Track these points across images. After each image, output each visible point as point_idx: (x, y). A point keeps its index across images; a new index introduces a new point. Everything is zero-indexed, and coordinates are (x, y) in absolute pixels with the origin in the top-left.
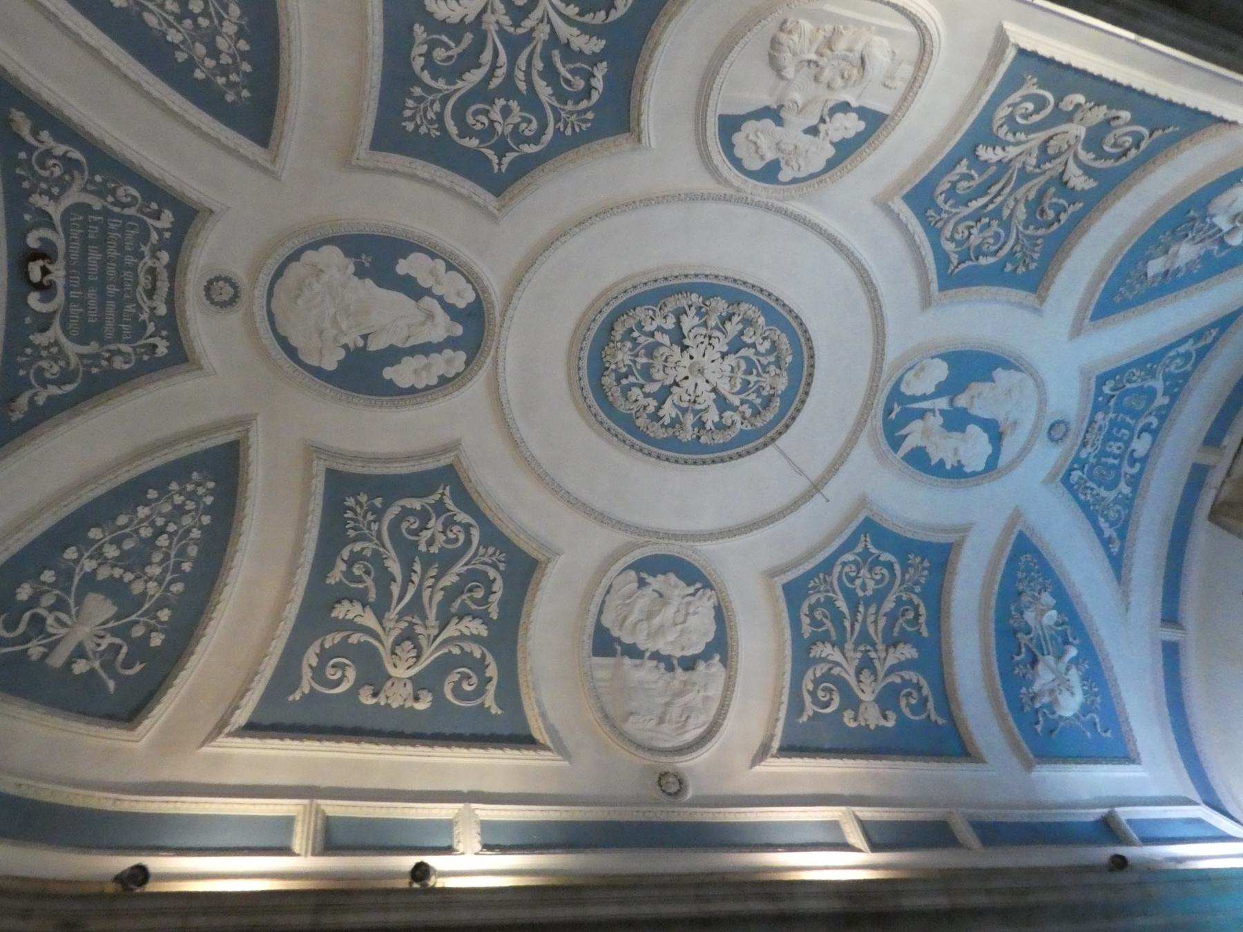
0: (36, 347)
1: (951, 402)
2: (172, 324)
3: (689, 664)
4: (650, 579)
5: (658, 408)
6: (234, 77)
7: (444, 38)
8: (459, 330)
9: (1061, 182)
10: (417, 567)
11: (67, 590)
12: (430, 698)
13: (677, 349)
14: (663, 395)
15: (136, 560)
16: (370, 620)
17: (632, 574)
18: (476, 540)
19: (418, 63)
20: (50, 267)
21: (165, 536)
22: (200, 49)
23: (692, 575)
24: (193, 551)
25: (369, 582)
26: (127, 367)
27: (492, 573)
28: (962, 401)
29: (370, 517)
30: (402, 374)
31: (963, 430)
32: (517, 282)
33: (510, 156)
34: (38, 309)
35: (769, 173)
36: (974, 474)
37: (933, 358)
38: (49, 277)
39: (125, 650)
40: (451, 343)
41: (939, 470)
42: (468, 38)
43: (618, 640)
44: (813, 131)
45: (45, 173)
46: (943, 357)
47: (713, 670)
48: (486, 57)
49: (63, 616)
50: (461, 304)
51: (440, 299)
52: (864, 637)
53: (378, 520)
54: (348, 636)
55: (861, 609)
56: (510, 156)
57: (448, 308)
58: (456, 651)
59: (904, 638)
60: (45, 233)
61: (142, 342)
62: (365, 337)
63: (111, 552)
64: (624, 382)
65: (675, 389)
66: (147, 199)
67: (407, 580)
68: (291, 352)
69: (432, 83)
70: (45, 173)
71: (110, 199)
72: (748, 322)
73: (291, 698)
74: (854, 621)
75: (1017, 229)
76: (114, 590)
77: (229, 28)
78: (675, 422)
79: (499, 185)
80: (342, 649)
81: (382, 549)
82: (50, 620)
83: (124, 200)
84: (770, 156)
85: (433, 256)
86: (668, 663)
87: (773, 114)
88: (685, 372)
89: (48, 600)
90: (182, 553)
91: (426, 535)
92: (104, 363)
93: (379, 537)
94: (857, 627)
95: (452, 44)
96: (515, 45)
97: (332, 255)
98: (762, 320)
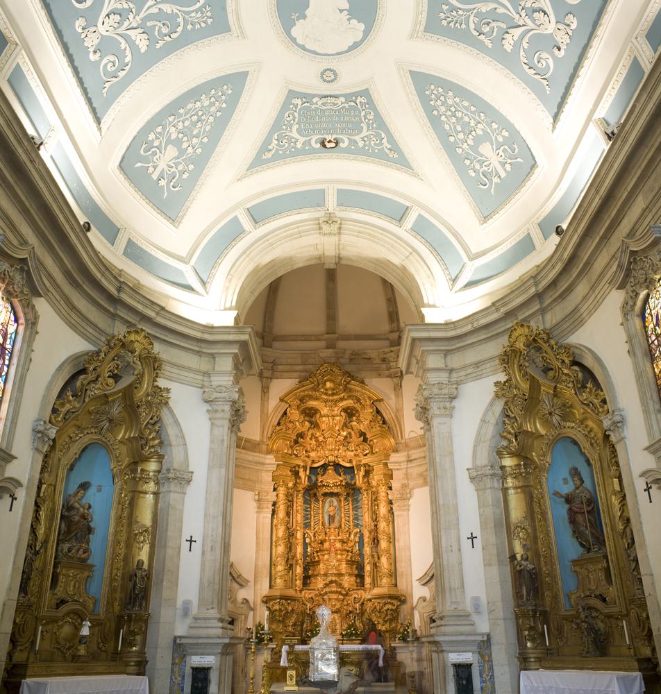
0: (365, 146)
2: (349, 97)
6: (220, 94)
7: (156, 33)
11: (475, 158)
12: (571, 16)
15: (468, 130)
20: (328, 140)
21: (457, 112)
22: (213, 109)
24: (466, 104)
25: (493, 24)
26: (372, 114)
29: (455, 13)
34: (347, 144)
38: (332, 140)
39: (507, 147)
42: (149, 24)
45: (287, 145)
48: (154, 10)
49: (485, 164)
53: (457, 9)
54: (524, 48)
60: (313, 143)
61: (359, 107)
62: (341, 11)
63: (461, 136)
66: (289, 109)
68: (355, 46)
69: (182, 24)
70: (287, 145)
71: (292, 122)
73: (548, 92)
76: (478, 141)
77: (198, 104)
80: (530, 53)
81: (475, 11)
82: (486, 169)
83: (291, 118)
89: (478, 166)
90: (466, 108)
92: (371, 121)
93: (468, 10)
95: (157, 28)
97: (295, 32)
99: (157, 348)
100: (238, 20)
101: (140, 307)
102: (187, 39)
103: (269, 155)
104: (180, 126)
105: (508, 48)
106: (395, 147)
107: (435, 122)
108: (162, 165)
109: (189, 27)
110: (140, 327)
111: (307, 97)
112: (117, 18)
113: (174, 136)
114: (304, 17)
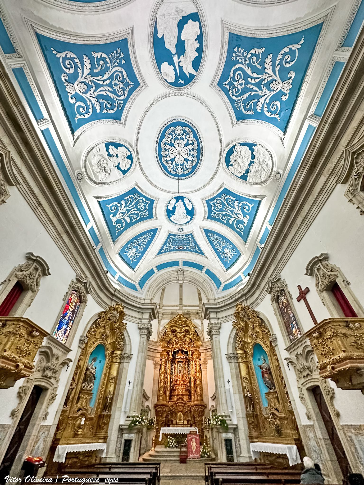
1: (174, 55)
2: (186, 235)
3: (253, 157)
4: (231, 163)
5: (190, 161)
8: (180, 200)
9: (91, 74)
10: (224, 209)
13: (175, 159)
14: (187, 160)
15: (220, 244)
16: (233, 219)
17: (230, 167)
18: (220, 199)
19: (138, 219)
22: (147, 238)
23: (230, 152)
24: (220, 238)
27: (226, 197)
28: (173, 51)
30: (190, 208)
31: (184, 41)
32: (169, 192)
33: (147, 201)
35: (130, 157)
36: (200, 28)
37: (161, 73)
40: (183, 201)
41: (200, 50)
43: (244, 174)
44: (117, 156)
46: (159, 67)
47: (256, 150)
48: (133, 212)
50: (176, 200)
51: (175, 204)
52: (258, 85)
53: (216, 213)
55: (248, 86)
56: (147, 201)
57: (177, 202)
58: (240, 208)
59: (262, 63)
63: (219, 246)
64: (185, 169)
65: (185, 158)
67: (227, 211)
68: (188, 222)
72: (165, 144)
74: (252, 90)
75: (111, 70)
78: (193, 156)
79: (153, 201)
84: (126, 159)
85: (168, 206)
86: (252, 163)
87: (118, 167)
88: (180, 156)
89: (224, 255)
91: (219, 207)
94: (255, 88)
96: (128, 211)
97: (171, 218)
98: (164, 140)
99: (125, 310)
100: (156, 215)
101: (121, 297)
102: (141, 220)
103: (163, 251)
104: (138, 243)
105: (231, 223)
106: (200, 249)
107: (211, 243)
108: (131, 254)
109: (142, 217)
110: (120, 303)
111: (175, 235)
112: (122, 214)
113: (135, 246)
114: (174, 215)
